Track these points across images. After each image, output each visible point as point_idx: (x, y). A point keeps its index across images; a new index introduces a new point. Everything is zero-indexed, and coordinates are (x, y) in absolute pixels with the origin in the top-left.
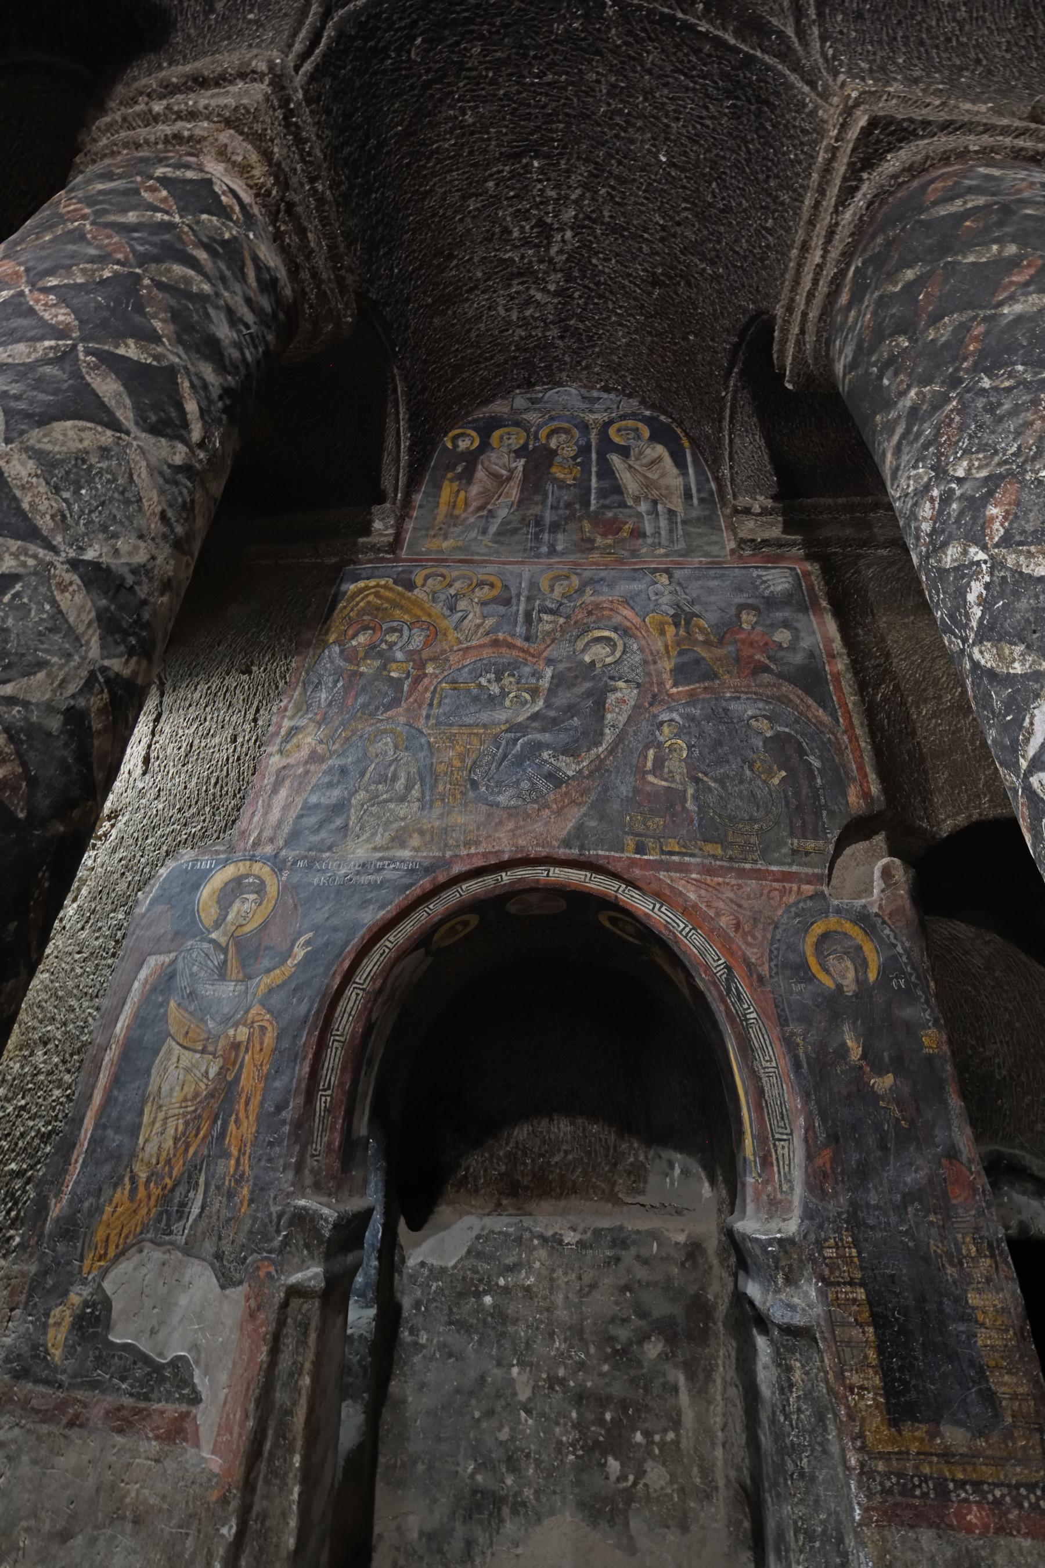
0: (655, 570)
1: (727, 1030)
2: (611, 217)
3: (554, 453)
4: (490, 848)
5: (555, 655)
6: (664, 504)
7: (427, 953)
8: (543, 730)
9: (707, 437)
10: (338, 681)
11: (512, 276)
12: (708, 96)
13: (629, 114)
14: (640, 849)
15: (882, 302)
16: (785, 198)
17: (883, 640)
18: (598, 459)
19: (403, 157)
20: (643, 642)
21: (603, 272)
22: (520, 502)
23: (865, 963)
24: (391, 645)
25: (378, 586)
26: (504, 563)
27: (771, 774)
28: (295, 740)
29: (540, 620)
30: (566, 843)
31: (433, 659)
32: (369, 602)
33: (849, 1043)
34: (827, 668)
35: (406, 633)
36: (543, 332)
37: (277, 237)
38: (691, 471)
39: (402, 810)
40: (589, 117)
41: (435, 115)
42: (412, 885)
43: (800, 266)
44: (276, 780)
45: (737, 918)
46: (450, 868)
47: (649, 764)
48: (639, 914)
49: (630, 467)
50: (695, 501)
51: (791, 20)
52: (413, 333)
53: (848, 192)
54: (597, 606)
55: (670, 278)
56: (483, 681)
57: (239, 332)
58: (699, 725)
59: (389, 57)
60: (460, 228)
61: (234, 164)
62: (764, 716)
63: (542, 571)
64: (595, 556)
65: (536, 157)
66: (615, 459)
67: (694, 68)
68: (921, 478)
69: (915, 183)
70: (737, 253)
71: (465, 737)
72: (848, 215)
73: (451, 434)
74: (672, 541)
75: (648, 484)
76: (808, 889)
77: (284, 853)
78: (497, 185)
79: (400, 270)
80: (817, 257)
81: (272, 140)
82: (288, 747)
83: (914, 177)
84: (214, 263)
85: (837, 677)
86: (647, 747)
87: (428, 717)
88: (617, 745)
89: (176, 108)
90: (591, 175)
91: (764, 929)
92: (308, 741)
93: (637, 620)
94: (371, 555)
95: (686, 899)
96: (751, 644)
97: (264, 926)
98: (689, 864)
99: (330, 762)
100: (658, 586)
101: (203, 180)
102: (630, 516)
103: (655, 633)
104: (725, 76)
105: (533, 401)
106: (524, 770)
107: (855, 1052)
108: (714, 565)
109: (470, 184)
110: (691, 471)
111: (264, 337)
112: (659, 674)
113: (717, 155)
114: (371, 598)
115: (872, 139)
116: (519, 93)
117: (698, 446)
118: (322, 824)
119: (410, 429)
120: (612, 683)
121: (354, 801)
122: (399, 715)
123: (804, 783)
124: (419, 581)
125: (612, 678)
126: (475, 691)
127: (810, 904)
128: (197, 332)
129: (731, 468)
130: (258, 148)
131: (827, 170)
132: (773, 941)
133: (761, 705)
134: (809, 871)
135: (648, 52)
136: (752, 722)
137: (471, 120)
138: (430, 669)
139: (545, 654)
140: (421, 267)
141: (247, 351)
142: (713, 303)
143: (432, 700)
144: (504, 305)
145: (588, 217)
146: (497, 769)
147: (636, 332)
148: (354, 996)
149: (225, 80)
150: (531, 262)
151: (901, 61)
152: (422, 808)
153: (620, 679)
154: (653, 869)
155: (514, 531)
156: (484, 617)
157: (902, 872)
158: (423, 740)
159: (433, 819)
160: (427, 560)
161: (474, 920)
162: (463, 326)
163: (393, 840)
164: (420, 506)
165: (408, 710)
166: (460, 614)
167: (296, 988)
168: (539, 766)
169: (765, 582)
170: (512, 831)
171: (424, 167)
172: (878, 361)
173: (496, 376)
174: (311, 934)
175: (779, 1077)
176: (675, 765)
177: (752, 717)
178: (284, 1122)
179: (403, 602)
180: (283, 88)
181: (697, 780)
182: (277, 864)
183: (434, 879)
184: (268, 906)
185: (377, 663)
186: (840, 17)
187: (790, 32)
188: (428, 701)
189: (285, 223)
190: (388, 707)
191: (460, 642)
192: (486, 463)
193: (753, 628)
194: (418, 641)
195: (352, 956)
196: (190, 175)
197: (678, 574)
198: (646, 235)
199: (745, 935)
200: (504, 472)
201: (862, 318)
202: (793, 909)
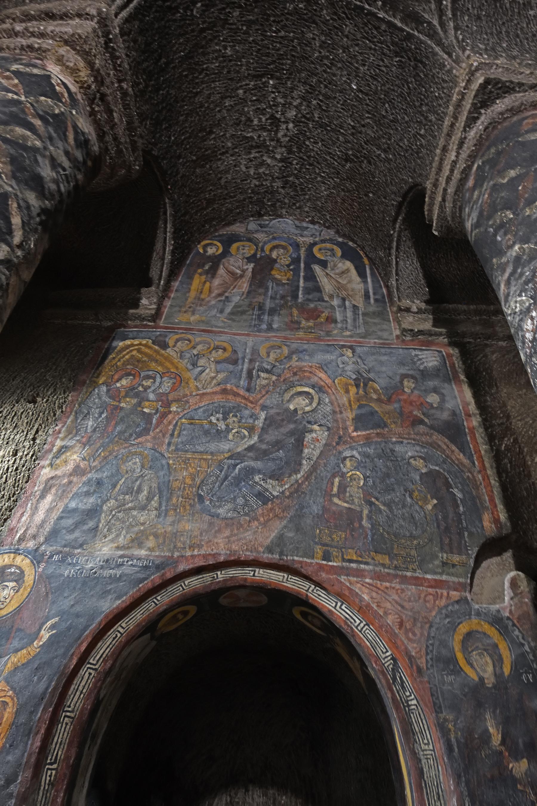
0: (343, 346)
1: (394, 715)
2: (319, 118)
3: (275, 261)
4: (209, 551)
5: (268, 403)
7: (152, 638)
8: (256, 459)
9: (381, 259)
10: (103, 413)
11: (252, 147)
12: (384, 54)
13: (333, 59)
14: (327, 557)
15: (496, 188)
16: (433, 118)
17: (504, 405)
18: (305, 268)
19: (183, 71)
20: (333, 397)
21: (313, 150)
22: (249, 292)
23: (501, 659)
24: (146, 388)
25: (140, 344)
26: (234, 334)
27: (426, 501)
28: (63, 457)
29: (259, 376)
30: (270, 550)
31: (177, 401)
32: (133, 356)
33: (491, 730)
34: (465, 423)
35: (158, 380)
36: (271, 183)
37: (92, 113)
38: (369, 280)
39: (142, 517)
40: (307, 58)
41: (207, 48)
42: (146, 579)
43: (442, 160)
44: (45, 488)
45: (400, 617)
47: (335, 489)
48: (324, 610)
49: (327, 274)
50: (372, 301)
51: (436, 17)
52: (182, 177)
53: (472, 120)
54: (301, 369)
55: (357, 158)
57: (58, 172)
58: (372, 461)
59: (179, 12)
60: (218, 116)
61: (67, 67)
62: (420, 457)
64: (301, 334)
65: (272, 78)
66: (317, 268)
67: (375, 37)
68: (524, 303)
69: (515, 119)
70: (401, 147)
72: (472, 134)
73: (203, 243)
75: (340, 287)
76: (455, 595)
77: (43, 548)
78: (245, 92)
79: (176, 138)
80: (452, 156)
81: (95, 56)
82: (58, 461)
83: (514, 114)
84: (46, 128)
85: (472, 430)
86: (334, 476)
87: (169, 444)
88: (311, 473)
89: (31, 30)
90: (307, 92)
91: (422, 627)
92: (74, 458)
93: (329, 381)
94: (138, 322)
95: (361, 600)
96: (411, 403)
97: (19, 610)
98: (364, 570)
99: (89, 475)
100: (345, 358)
101: (45, 75)
102: (326, 308)
103: (342, 391)
104: (393, 43)
105: (261, 226)
106: (240, 490)
107: (496, 739)
108: (384, 345)
109: (227, 90)
110: (369, 280)
111: (75, 176)
112: (344, 421)
113: (388, 88)
114: (134, 353)
115: (487, 91)
116: (262, 40)
117: (374, 264)
118: (77, 525)
119: (174, 238)
120: (309, 426)
121: (105, 508)
122: (147, 441)
123: (450, 510)
124: (171, 343)
125: (309, 422)
126: (207, 427)
127: (457, 607)
128: (27, 171)
129: (397, 280)
130: (85, 60)
131: (459, 105)
132: (429, 637)
133: (418, 448)
134: (456, 580)
135: (346, 25)
136: (412, 461)
137: (230, 53)
138: (174, 408)
140: (190, 137)
141: (62, 186)
142: (385, 176)
143: (173, 431)
144: (245, 165)
145: (304, 117)
147: (334, 188)
148: (87, 675)
149: (67, 16)
150: (265, 140)
151: (505, 45)
152: (158, 516)
153: (315, 423)
154: (336, 574)
155: (243, 312)
156: (218, 372)
157: (525, 583)
158: (164, 462)
159: (166, 525)
160: (179, 329)
161: (193, 610)
162: (216, 175)
163: (133, 541)
164: (176, 291)
165: (154, 438)
166: (200, 369)
167: (37, 666)
168: (252, 487)
169: (420, 359)
170: (227, 537)
171: (197, 78)
172: (493, 224)
173: (236, 209)
174: (57, 619)
175: (435, 759)
176: (355, 491)
177: (411, 457)
178: (10, 796)
179: (158, 357)
180: (106, 26)
181: (371, 504)
182: (36, 557)
183: (163, 575)
184: (24, 593)
185: (134, 401)
186: (466, 18)
187: (435, 22)
188: (170, 432)
189: (98, 105)
190: (139, 435)
191: (198, 389)
192: (227, 264)
193: (412, 392)
194: (166, 386)
195: (90, 639)
196: (36, 71)
197: (359, 350)
198: (342, 131)
199: (407, 631)
200: (238, 271)
201: (483, 196)
202: (444, 611)
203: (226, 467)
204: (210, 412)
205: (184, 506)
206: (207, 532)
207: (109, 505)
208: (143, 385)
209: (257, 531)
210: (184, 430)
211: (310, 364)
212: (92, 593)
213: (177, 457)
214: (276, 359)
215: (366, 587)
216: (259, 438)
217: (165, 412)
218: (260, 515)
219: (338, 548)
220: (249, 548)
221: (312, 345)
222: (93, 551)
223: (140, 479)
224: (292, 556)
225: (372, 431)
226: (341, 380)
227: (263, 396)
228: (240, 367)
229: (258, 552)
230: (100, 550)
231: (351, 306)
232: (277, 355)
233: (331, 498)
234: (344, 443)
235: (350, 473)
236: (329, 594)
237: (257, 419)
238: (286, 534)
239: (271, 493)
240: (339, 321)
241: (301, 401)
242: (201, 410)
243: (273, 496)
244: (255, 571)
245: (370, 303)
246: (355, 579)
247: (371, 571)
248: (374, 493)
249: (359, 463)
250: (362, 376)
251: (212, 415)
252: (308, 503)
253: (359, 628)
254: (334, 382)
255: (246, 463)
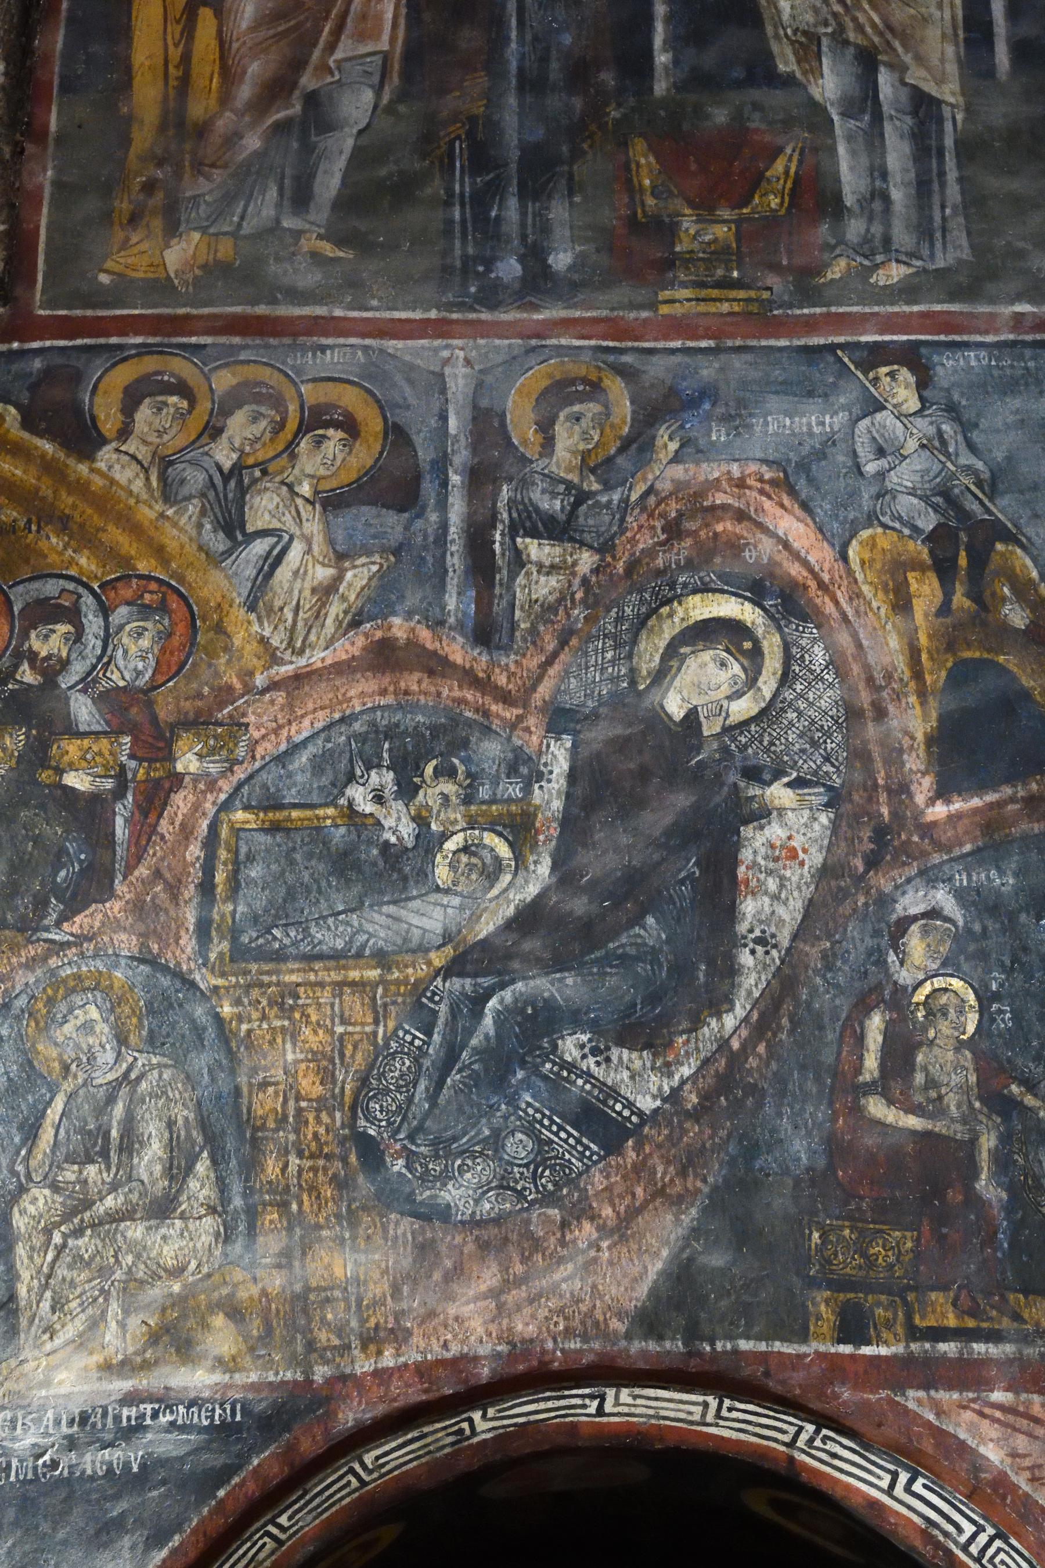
0: (875, 356)
4: (436, 1352)
5: (575, 693)
6: (899, 68)
8: (558, 964)
14: (853, 1327)
20: (844, 639)
22: (413, 56)
24: (52, 670)
29: (518, 561)
30: (648, 1321)
31: (197, 723)
35: (93, 623)
39: (168, 1242)
46: (331, 1415)
47: (871, 1062)
54: (696, 503)
56: (359, 796)
58: (1011, 926)
63: (513, 363)
64: (680, 299)
71: (325, 996)
74: (924, 230)
86: (863, 1007)
87: (203, 930)
95: (977, 1464)
98: (985, 1362)
102: (788, 123)
103: (880, 603)
106: (513, 1101)
112: (894, 756)
120: (754, 791)
121: (19, 1222)
124: (109, 420)
125: (753, 774)
126: (339, 834)
138: (188, 762)
139: (544, 690)
143: (209, 870)
146: (433, 1097)
152: (227, 1236)
153: (778, 774)
155: (402, 191)
156: (341, 557)
158: (199, 1012)
159: (262, 1271)
160: (126, 325)
163: (154, 1338)
165: (138, 907)
166: (260, 547)
168: (555, 1084)
170: (495, 1294)
176: (946, 1064)
179: (67, 501)
181: (1003, 1106)
183: (291, 1448)
188: (196, 874)
190: (74, 905)
194: (135, 655)
197: (948, 368)
203: (443, 1009)
204: (343, 765)
205: (313, 1189)
206: (413, 1279)
207: (32, 1209)
208: (32, 657)
209: (595, 1260)
210: (250, 858)
211: (735, 469)
212: (61, 1535)
213: (248, 987)
214: (585, 455)
215: (998, 1421)
216: (554, 867)
217: (157, 782)
218: (597, 1194)
219: (889, 1294)
220: (576, 1323)
221: (738, 362)
222: (22, 1386)
223: (124, 1091)
224: (731, 1337)
225: (1008, 791)
226: (872, 544)
227: (550, 662)
228: (434, 517)
229: (606, 1335)
230: (47, 1383)
231: (904, 95)
232: (586, 437)
233: (856, 1100)
234: (895, 858)
235: (927, 988)
236: (867, 1447)
237: (540, 776)
238: (703, 1259)
239: (630, 1105)
240: (849, 200)
241: (712, 668)
242: (303, 758)
243: (640, 1114)
244: (602, 1398)
245: (990, 72)
246: (956, 1396)
247: (1010, 1361)
248: (1019, 1061)
249: (962, 938)
250: (963, 514)
251: (351, 778)
252: (773, 1131)
253: (974, 1549)
254: (844, 557)
255: (519, 986)
